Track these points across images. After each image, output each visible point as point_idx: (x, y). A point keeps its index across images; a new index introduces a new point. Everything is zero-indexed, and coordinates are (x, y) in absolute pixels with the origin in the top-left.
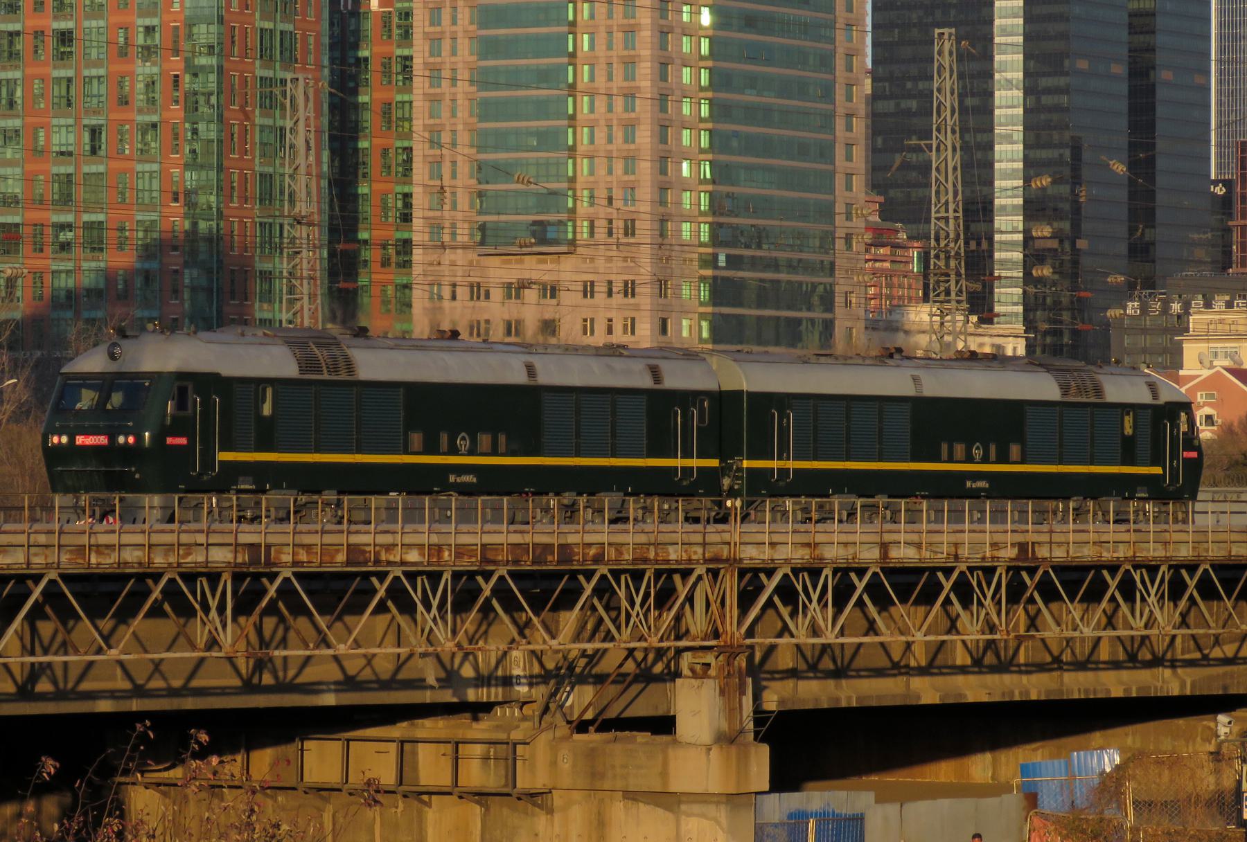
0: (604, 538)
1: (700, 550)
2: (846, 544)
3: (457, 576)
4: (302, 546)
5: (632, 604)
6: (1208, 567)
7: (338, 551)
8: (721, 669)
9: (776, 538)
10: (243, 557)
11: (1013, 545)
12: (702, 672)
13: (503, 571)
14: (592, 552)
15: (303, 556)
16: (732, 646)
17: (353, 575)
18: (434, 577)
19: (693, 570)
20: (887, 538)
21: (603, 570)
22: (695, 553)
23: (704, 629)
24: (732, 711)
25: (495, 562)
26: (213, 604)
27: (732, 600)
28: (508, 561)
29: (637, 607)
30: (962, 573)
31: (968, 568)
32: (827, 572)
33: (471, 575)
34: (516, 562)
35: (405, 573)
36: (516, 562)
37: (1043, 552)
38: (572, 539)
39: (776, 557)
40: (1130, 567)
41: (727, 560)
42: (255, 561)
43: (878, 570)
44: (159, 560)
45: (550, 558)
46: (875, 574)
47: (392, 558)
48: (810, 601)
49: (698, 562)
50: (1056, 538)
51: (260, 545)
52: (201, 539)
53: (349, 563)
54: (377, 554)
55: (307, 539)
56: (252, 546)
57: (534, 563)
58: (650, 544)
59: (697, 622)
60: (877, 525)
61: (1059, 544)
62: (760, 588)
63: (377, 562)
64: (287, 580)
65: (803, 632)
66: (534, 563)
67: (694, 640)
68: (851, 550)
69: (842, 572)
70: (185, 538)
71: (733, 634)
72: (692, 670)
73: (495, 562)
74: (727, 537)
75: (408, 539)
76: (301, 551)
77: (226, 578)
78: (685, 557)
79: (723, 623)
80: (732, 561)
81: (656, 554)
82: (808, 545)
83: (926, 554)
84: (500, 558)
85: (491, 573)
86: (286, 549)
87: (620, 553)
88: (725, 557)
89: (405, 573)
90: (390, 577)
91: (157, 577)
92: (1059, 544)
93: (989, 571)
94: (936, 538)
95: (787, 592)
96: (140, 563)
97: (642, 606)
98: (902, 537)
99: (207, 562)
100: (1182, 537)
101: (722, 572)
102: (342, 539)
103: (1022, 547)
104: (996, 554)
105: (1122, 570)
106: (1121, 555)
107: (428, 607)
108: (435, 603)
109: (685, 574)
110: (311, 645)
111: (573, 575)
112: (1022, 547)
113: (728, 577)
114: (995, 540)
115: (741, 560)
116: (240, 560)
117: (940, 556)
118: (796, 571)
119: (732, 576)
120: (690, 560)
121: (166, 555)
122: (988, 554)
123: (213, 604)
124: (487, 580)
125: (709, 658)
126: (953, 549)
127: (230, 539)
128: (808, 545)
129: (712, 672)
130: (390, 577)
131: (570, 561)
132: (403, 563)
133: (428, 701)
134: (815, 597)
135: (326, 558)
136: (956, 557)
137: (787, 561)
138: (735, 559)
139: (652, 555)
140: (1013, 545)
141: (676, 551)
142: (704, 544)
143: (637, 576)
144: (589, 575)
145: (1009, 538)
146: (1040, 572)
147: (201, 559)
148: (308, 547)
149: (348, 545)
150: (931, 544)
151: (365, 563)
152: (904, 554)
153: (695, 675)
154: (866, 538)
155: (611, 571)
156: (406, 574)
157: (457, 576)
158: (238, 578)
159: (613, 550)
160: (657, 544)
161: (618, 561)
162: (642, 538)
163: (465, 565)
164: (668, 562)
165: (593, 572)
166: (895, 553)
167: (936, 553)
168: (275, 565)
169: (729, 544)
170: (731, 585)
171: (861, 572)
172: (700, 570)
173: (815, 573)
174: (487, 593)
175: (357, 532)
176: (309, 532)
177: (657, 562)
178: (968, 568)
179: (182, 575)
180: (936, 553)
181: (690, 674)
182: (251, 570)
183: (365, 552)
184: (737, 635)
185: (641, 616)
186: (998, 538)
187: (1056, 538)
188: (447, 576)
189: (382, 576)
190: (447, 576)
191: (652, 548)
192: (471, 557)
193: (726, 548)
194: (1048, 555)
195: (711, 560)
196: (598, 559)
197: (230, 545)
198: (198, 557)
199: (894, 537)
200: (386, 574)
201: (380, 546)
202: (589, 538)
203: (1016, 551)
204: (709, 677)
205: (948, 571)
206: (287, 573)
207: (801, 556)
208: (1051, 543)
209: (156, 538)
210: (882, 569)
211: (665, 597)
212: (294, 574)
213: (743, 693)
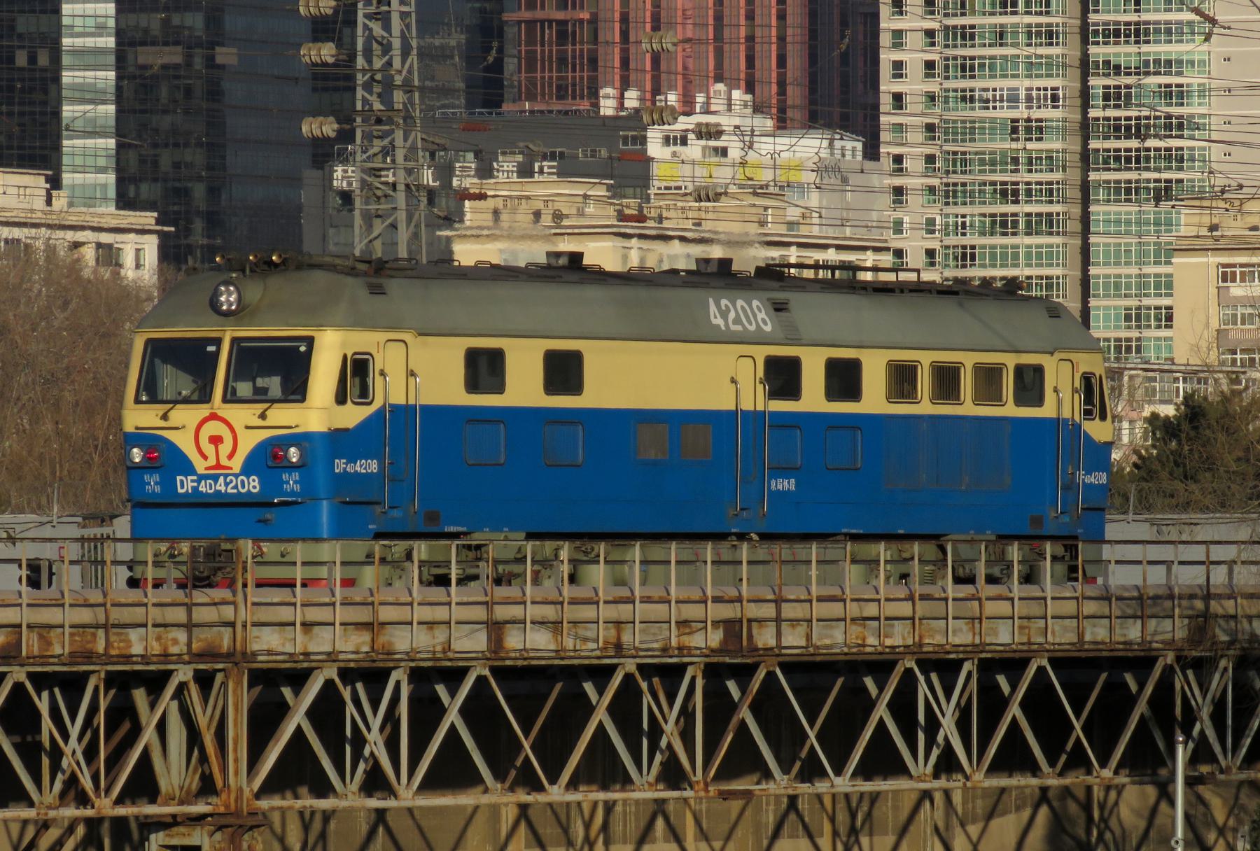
1: (182, 636)
2: (430, 624)
6: (1045, 662)
9: (314, 614)
11: (716, 624)
19: (171, 672)
20: (501, 612)
22: (175, 642)
30: (628, 677)
31: (640, 667)
37: (765, 638)
39: (311, 649)
40: (911, 663)
41: (229, 656)
46: (481, 680)
48: (369, 730)
49: (179, 659)
50: (789, 611)
58: (97, 627)
59: (173, 772)
61: (794, 622)
65: (355, 786)
67: (166, 804)
68: (440, 635)
69: (422, 677)
71: (240, 790)
74: (228, 612)
78: (156, 649)
79: (224, 769)
81: (108, 644)
82: (367, 626)
83: (569, 643)
88: (225, 649)
92: (794, 622)
93: (670, 674)
100: (1003, 608)
101: (219, 678)
103: (732, 627)
105: (899, 670)
106: (897, 641)
112: (732, 627)
114: (684, 616)
115: (254, 654)
117: (593, 646)
118: (347, 675)
119: (239, 683)
120: (165, 656)
122: (674, 643)
126: (613, 632)
128: (367, 626)
134: (376, 723)
136: (619, 647)
137: (331, 657)
138: (244, 653)
139: (100, 647)
142: (189, 626)
143: (72, 685)
146: (761, 674)
150: (575, 623)
152: (533, 643)
154: (458, 613)
155: (30, 675)
161: (43, 659)
162: (85, 616)
164: (127, 658)
166: (513, 641)
167: (585, 640)
169: (232, 625)
170: (238, 700)
171: (453, 676)
172: (184, 674)
177: (107, 658)
178: (640, 667)
180: (585, 640)
184: (247, 793)
187: (789, 611)
191: (101, 633)
194: (772, 642)
199: (516, 611)
205: (601, 674)
207: (353, 645)
208: (778, 620)
210: (494, 670)
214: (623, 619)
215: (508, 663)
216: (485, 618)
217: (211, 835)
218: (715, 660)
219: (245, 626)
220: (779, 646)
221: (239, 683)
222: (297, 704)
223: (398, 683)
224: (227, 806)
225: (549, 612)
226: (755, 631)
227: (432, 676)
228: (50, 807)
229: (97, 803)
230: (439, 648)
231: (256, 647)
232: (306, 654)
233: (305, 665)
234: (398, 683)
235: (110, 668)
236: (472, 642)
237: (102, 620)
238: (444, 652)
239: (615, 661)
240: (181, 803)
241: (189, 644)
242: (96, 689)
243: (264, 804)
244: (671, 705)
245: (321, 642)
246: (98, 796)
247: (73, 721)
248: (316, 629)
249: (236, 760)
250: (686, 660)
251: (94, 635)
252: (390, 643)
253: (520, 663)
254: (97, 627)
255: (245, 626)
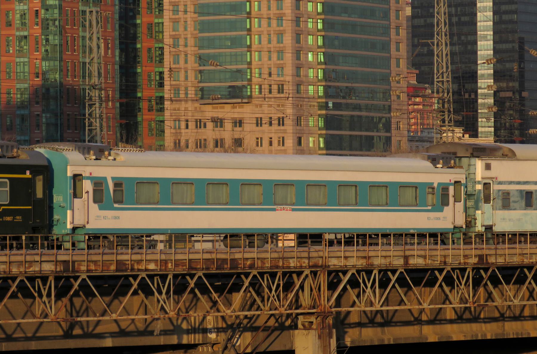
0: (255, 255)
2: (385, 257)
3: (175, 276)
4: (92, 261)
5: (270, 290)
7: (111, 264)
8: (319, 324)
9: (348, 254)
10: (60, 268)
11: (475, 256)
12: (308, 327)
13: (200, 274)
14: (249, 263)
15: (92, 267)
16: (324, 312)
17: (119, 277)
18: (164, 277)
20: (408, 253)
21: (254, 272)
22: (304, 262)
23: (310, 303)
24: (325, 347)
25: (196, 269)
26: (44, 293)
27: (324, 287)
28: (203, 268)
29: (273, 292)
30: (448, 271)
32: (375, 272)
33: (184, 276)
34: (207, 269)
35: (148, 276)
36: (207, 269)
37: (492, 260)
38: (238, 256)
41: (321, 266)
42: (66, 270)
43: (403, 271)
44: (15, 270)
45: (225, 266)
46: (401, 273)
47: (140, 267)
48: (367, 287)
49: (305, 267)
50: (499, 252)
51: (69, 261)
52: (37, 258)
53: (117, 270)
54: (132, 265)
55: (94, 258)
56: (65, 261)
57: (217, 269)
58: (280, 258)
59: (305, 299)
60: (402, 248)
61: (501, 255)
62: (340, 281)
63: (132, 269)
64: (84, 280)
65: (363, 304)
66: (217, 269)
67: (304, 309)
68: (388, 260)
70: (29, 258)
71: (325, 305)
72: (303, 325)
73: (196, 269)
74: (321, 254)
75: (149, 257)
76: (91, 264)
77: (51, 279)
78: (299, 265)
79: (320, 300)
80: (324, 267)
81: (283, 264)
82: (365, 257)
83: (430, 262)
84: (199, 267)
85: (194, 275)
86: (83, 263)
87: (263, 263)
88: (320, 265)
89: (147, 275)
90: (140, 278)
91: (14, 279)
92: (501, 255)
93: (463, 270)
94: (434, 253)
95: (354, 283)
96: (5, 272)
97: (276, 291)
98: (415, 253)
99: (41, 271)
102: (114, 257)
103: (481, 257)
104: (467, 261)
106: (534, 261)
107: (160, 293)
108: (164, 291)
109: (299, 274)
110: (98, 315)
111: (239, 275)
112: (481, 257)
113: (322, 275)
114: (466, 254)
115: (329, 266)
116: (58, 269)
117: (436, 262)
118: (359, 272)
119: (324, 274)
120: (301, 267)
121: (19, 267)
122: (462, 261)
123: (44, 293)
124: (192, 279)
125: (313, 319)
127: (53, 258)
128: (365, 257)
129: (314, 326)
130: (140, 278)
131: (237, 268)
132: (146, 270)
133: (162, 344)
134: (369, 286)
135: (105, 268)
136: (445, 263)
137: (354, 266)
138: (326, 266)
139: (281, 264)
140: (475, 256)
141: (294, 262)
142: (309, 258)
143: (273, 275)
144: (247, 275)
145: (473, 252)
146: (490, 270)
147: (37, 269)
148: (95, 262)
149: (117, 261)
150: (431, 256)
151: (126, 270)
152: (417, 262)
153: (305, 328)
154: (396, 253)
155: (259, 273)
156: (148, 276)
157: (175, 276)
158: (57, 279)
159: (260, 262)
160: (283, 258)
161: (262, 268)
162: (275, 255)
163: (180, 270)
164: (289, 267)
165: (250, 273)
166: (412, 261)
168: (78, 272)
169: (322, 257)
170: (323, 279)
171: (394, 272)
172: (307, 272)
173: (369, 272)
174: (192, 285)
175: (122, 254)
176: (96, 254)
177: (283, 268)
179: (28, 278)
181: (302, 327)
182: (65, 275)
183: (126, 264)
184: (327, 306)
185: (276, 297)
186: (467, 252)
187: (499, 252)
188: (170, 277)
189: (135, 277)
190: (170, 277)
191: (281, 260)
192: (183, 266)
193: (320, 260)
194: (494, 261)
195: (313, 266)
196: (252, 266)
197: (53, 261)
198: (36, 268)
200: (138, 275)
201: (135, 261)
202: (247, 255)
203: (477, 259)
204: (313, 329)
205: (441, 271)
206: (84, 276)
207: (361, 263)
208: (496, 254)
209: (13, 258)
210: (405, 270)
211: (288, 287)
212: (88, 276)
213: (331, 337)
214: (446, 254)
215: (410, 268)
216: (403, 255)
217: (316, 319)
218: (476, 266)
219: (326, 258)
220: (496, 263)
221: (324, 274)
222: (344, 279)
223: (375, 274)
224: (321, 310)
225: (422, 253)
226: (488, 258)
227: (384, 272)
228: (267, 311)
229: (280, 309)
230: (388, 264)
231: (330, 264)
232: (346, 266)
233: (346, 269)
234: (375, 274)
235: (283, 270)
236: (399, 262)
237: (281, 256)
238: (390, 264)
239: (444, 267)
240: (309, 309)
241: (309, 263)
242: (280, 276)
243: (333, 310)
244: (463, 279)
245: (351, 262)
246: (280, 307)
247: (273, 286)
248: (349, 259)
249: (324, 297)
250: (466, 266)
251: (279, 261)
252: (372, 262)
253: (413, 268)
254: (280, 258)
255: (326, 258)
